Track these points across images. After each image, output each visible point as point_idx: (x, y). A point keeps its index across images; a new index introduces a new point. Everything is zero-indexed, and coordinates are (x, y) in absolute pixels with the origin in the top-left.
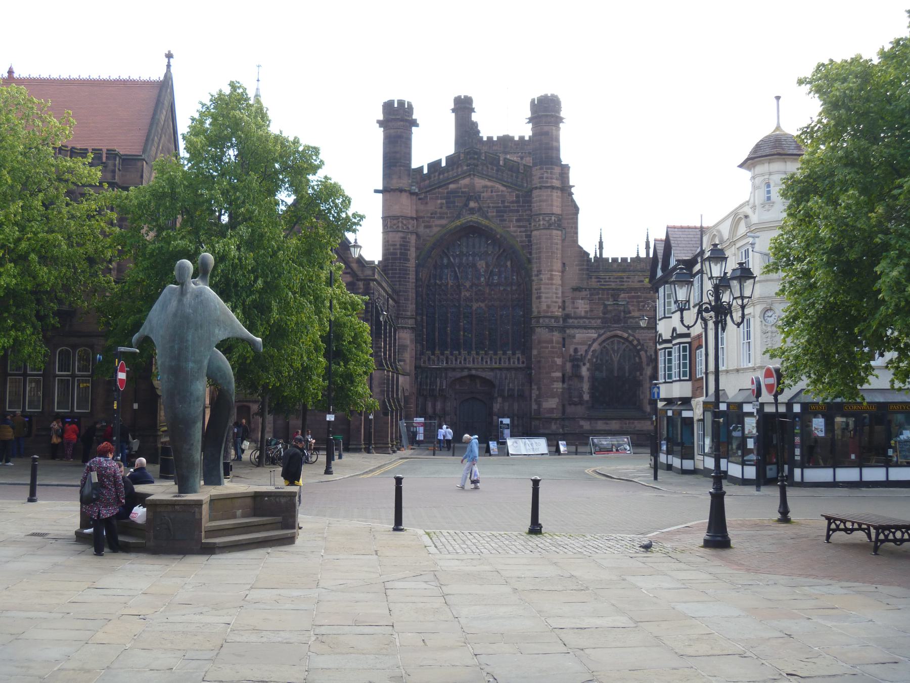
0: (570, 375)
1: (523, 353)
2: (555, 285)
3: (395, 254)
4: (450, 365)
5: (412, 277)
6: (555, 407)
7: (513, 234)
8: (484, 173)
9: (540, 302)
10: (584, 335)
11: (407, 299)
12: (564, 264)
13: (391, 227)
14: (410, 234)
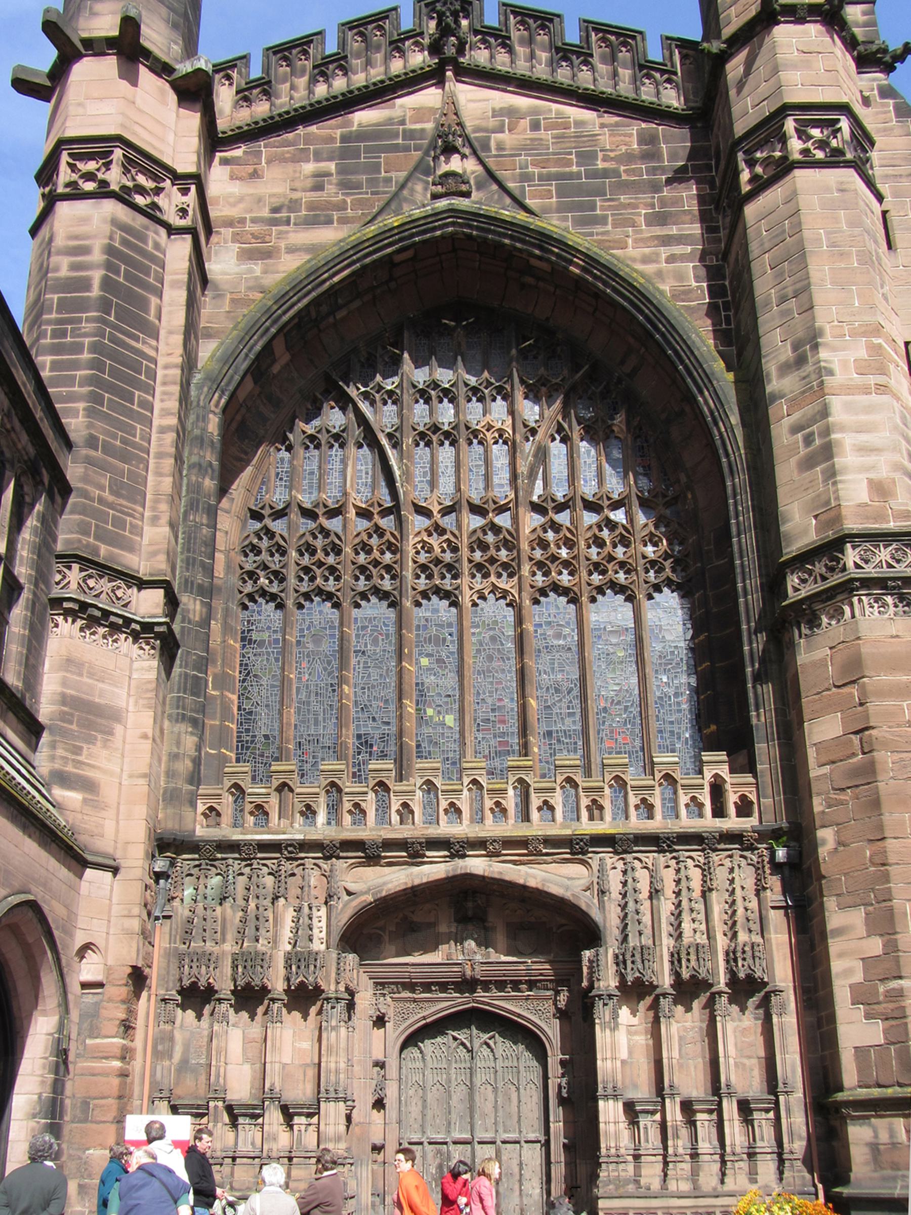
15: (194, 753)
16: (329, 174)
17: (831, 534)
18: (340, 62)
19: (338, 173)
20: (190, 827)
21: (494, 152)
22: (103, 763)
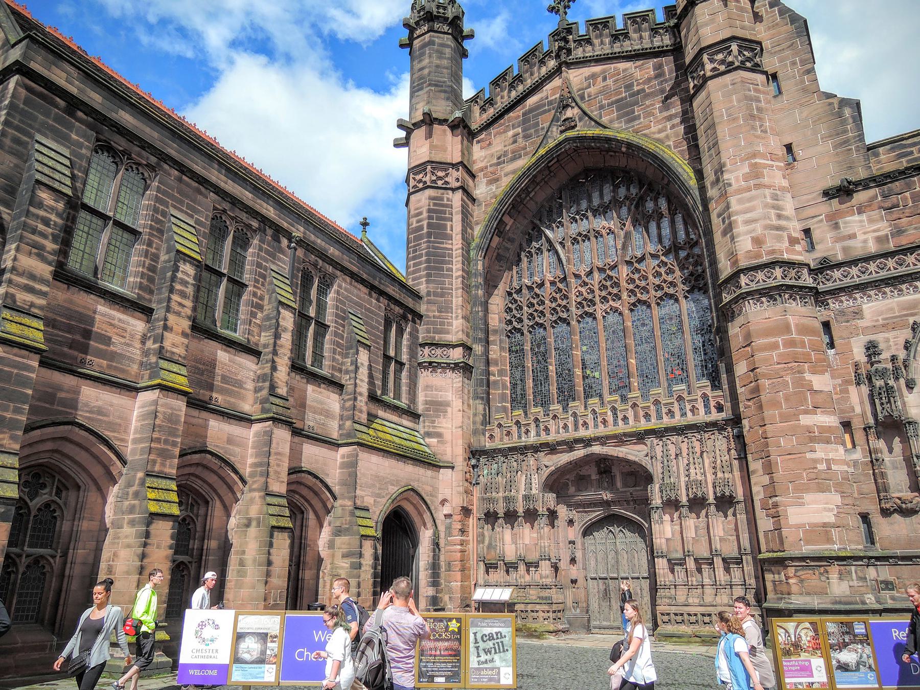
0: (871, 421)
1: (716, 384)
2: (769, 187)
3: (420, 228)
4: (544, 438)
5: (456, 267)
6: (832, 519)
7: (657, 136)
8: (587, 55)
9: (733, 238)
10: (887, 301)
11: (446, 308)
12: (789, 148)
13: (414, 187)
14: (450, 192)
15: (483, 412)
16: (519, 134)
17: (735, 270)
18: (519, 78)
19: (522, 132)
20: (483, 444)
21: (587, 99)
22: (444, 425)
